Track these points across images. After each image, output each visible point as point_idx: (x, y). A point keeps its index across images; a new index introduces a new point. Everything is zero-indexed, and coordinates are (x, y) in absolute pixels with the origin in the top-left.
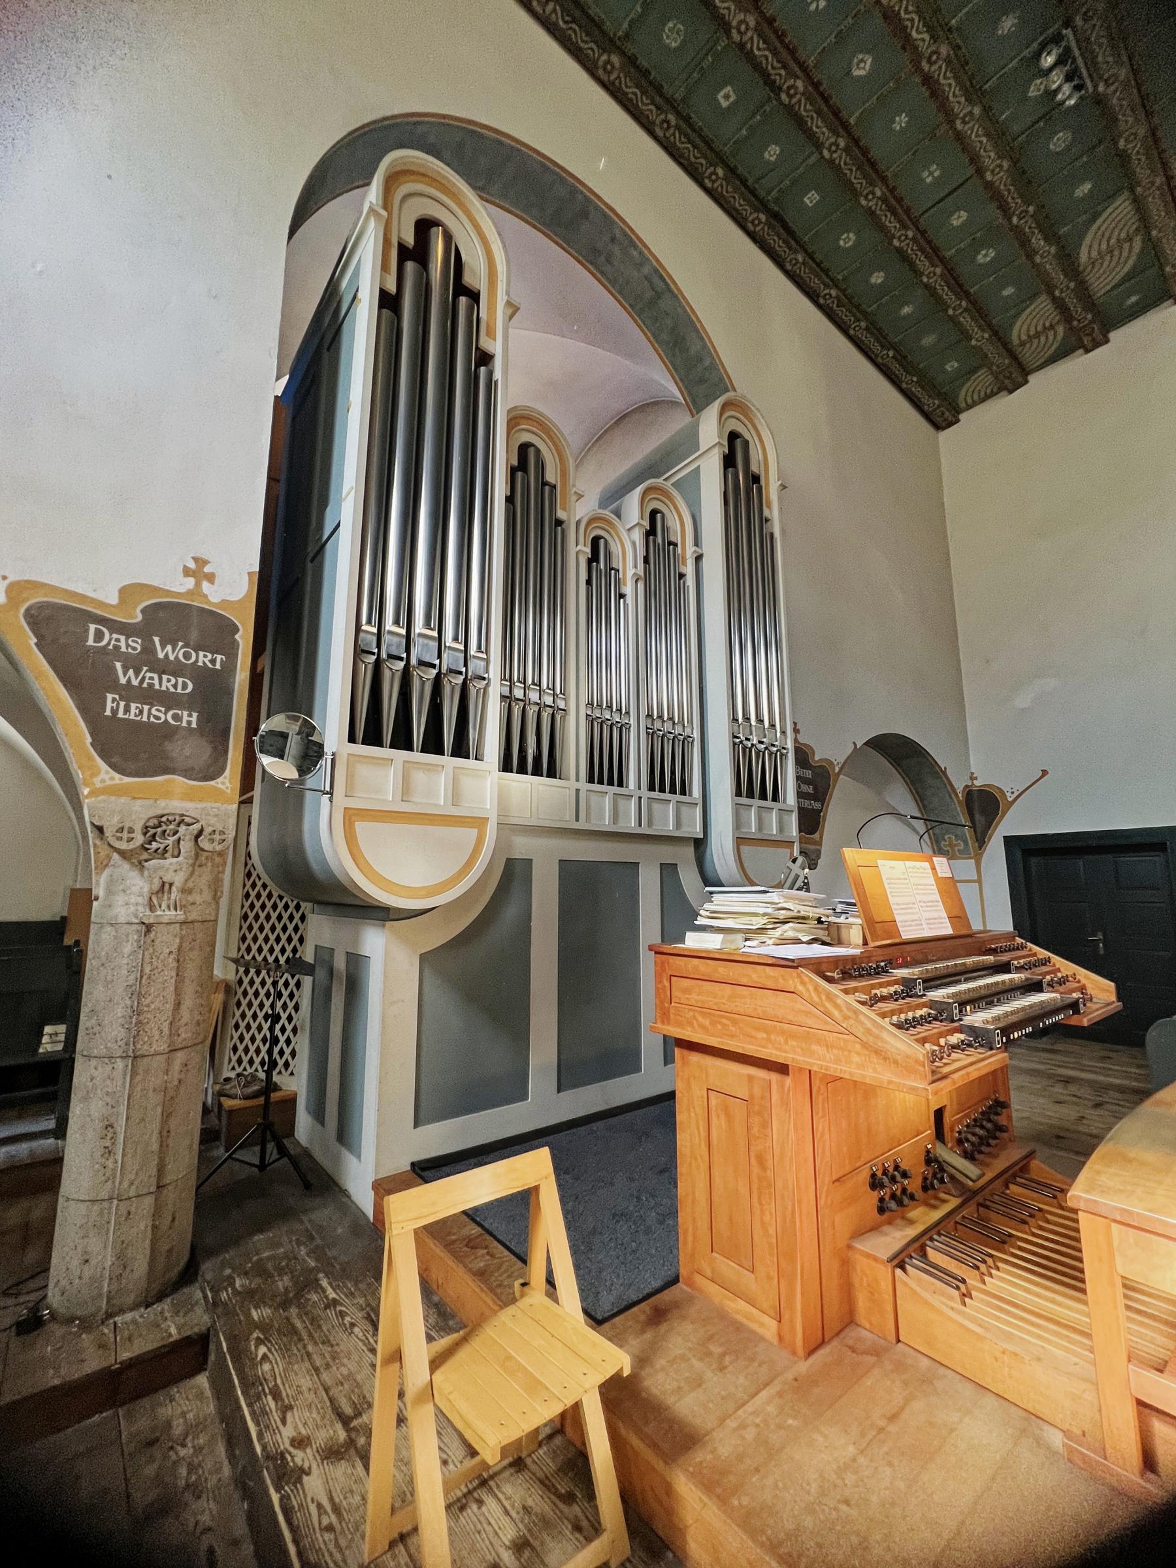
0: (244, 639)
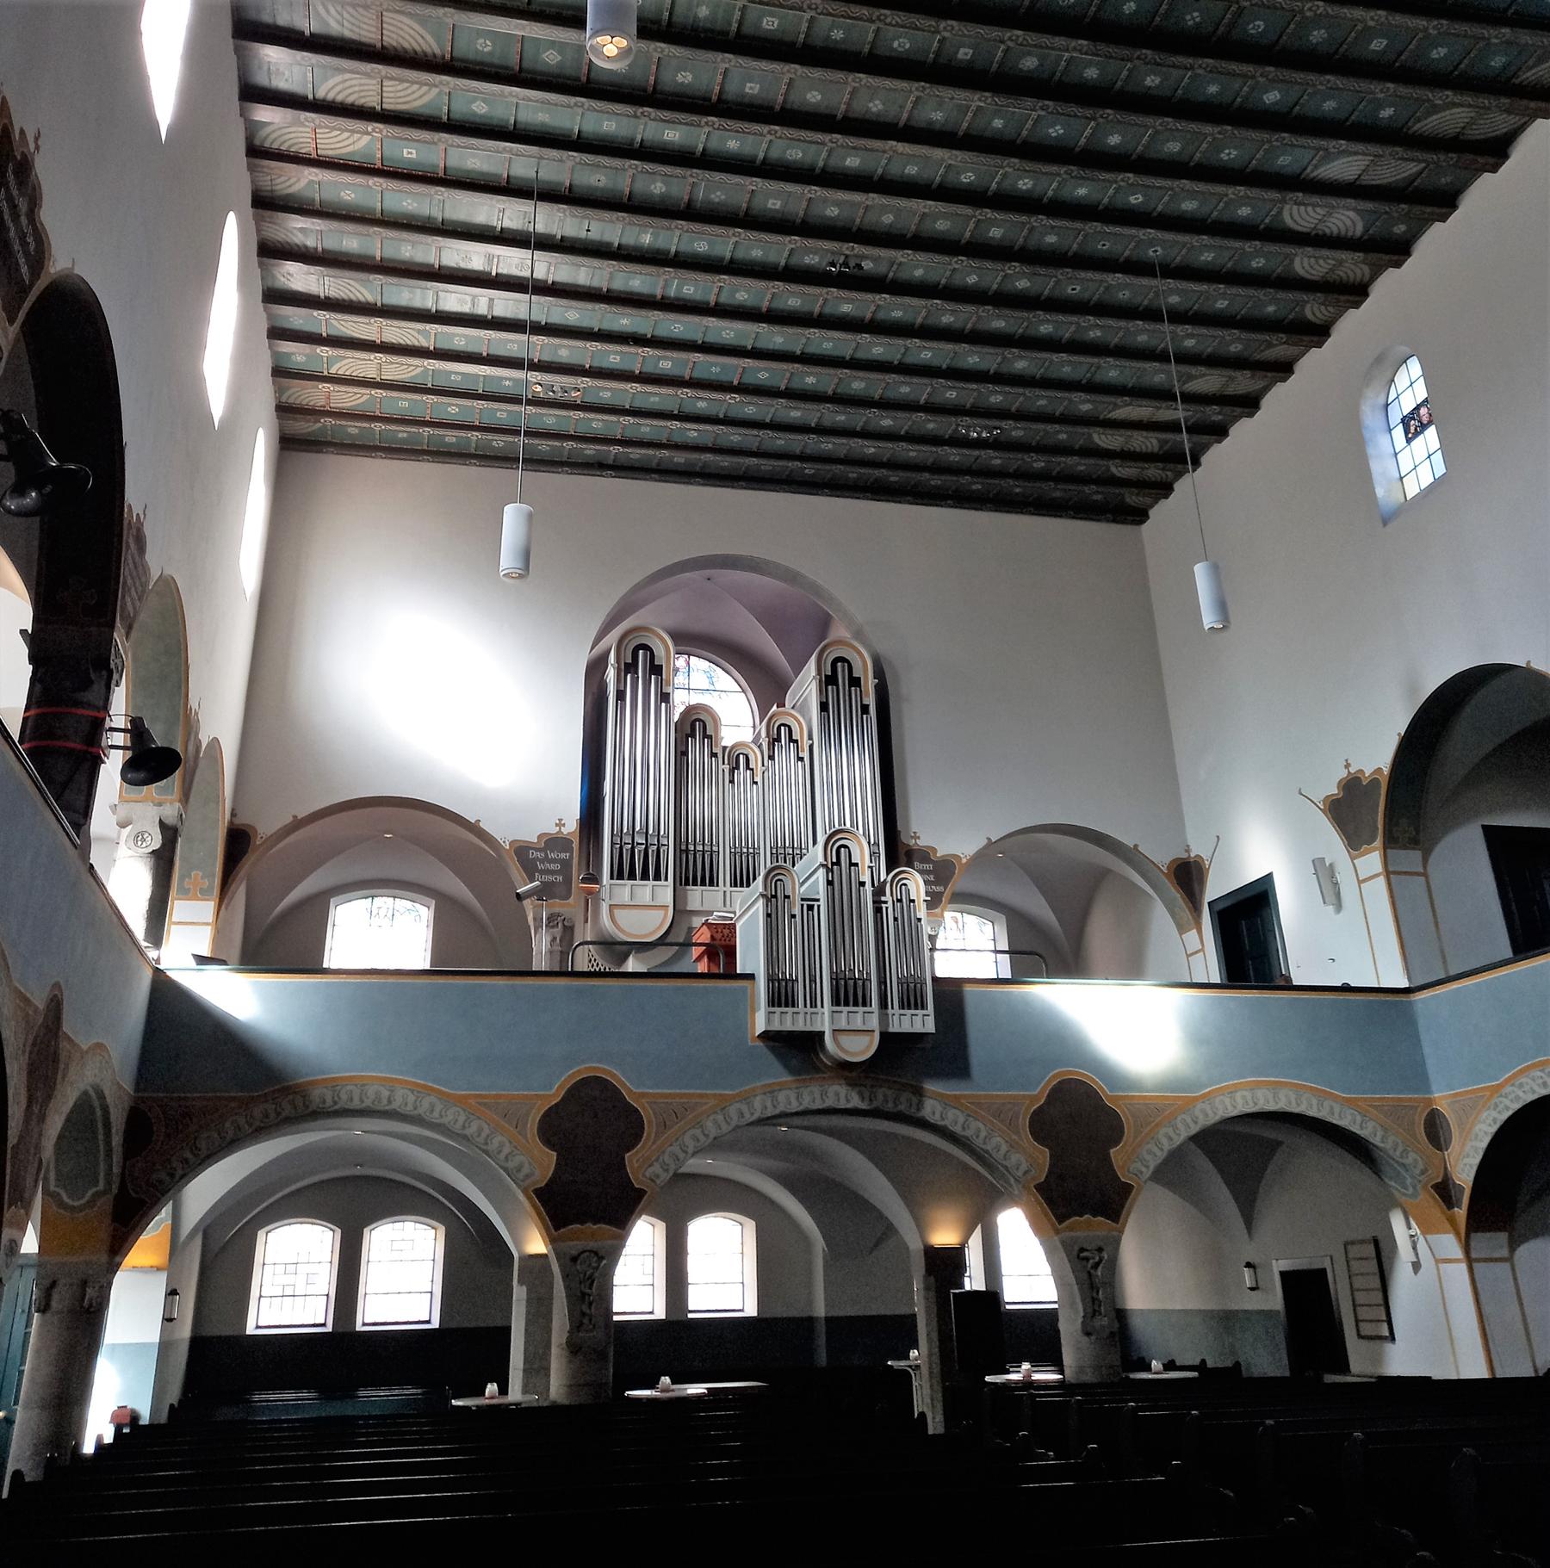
0: (576, 845)
